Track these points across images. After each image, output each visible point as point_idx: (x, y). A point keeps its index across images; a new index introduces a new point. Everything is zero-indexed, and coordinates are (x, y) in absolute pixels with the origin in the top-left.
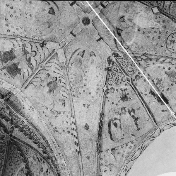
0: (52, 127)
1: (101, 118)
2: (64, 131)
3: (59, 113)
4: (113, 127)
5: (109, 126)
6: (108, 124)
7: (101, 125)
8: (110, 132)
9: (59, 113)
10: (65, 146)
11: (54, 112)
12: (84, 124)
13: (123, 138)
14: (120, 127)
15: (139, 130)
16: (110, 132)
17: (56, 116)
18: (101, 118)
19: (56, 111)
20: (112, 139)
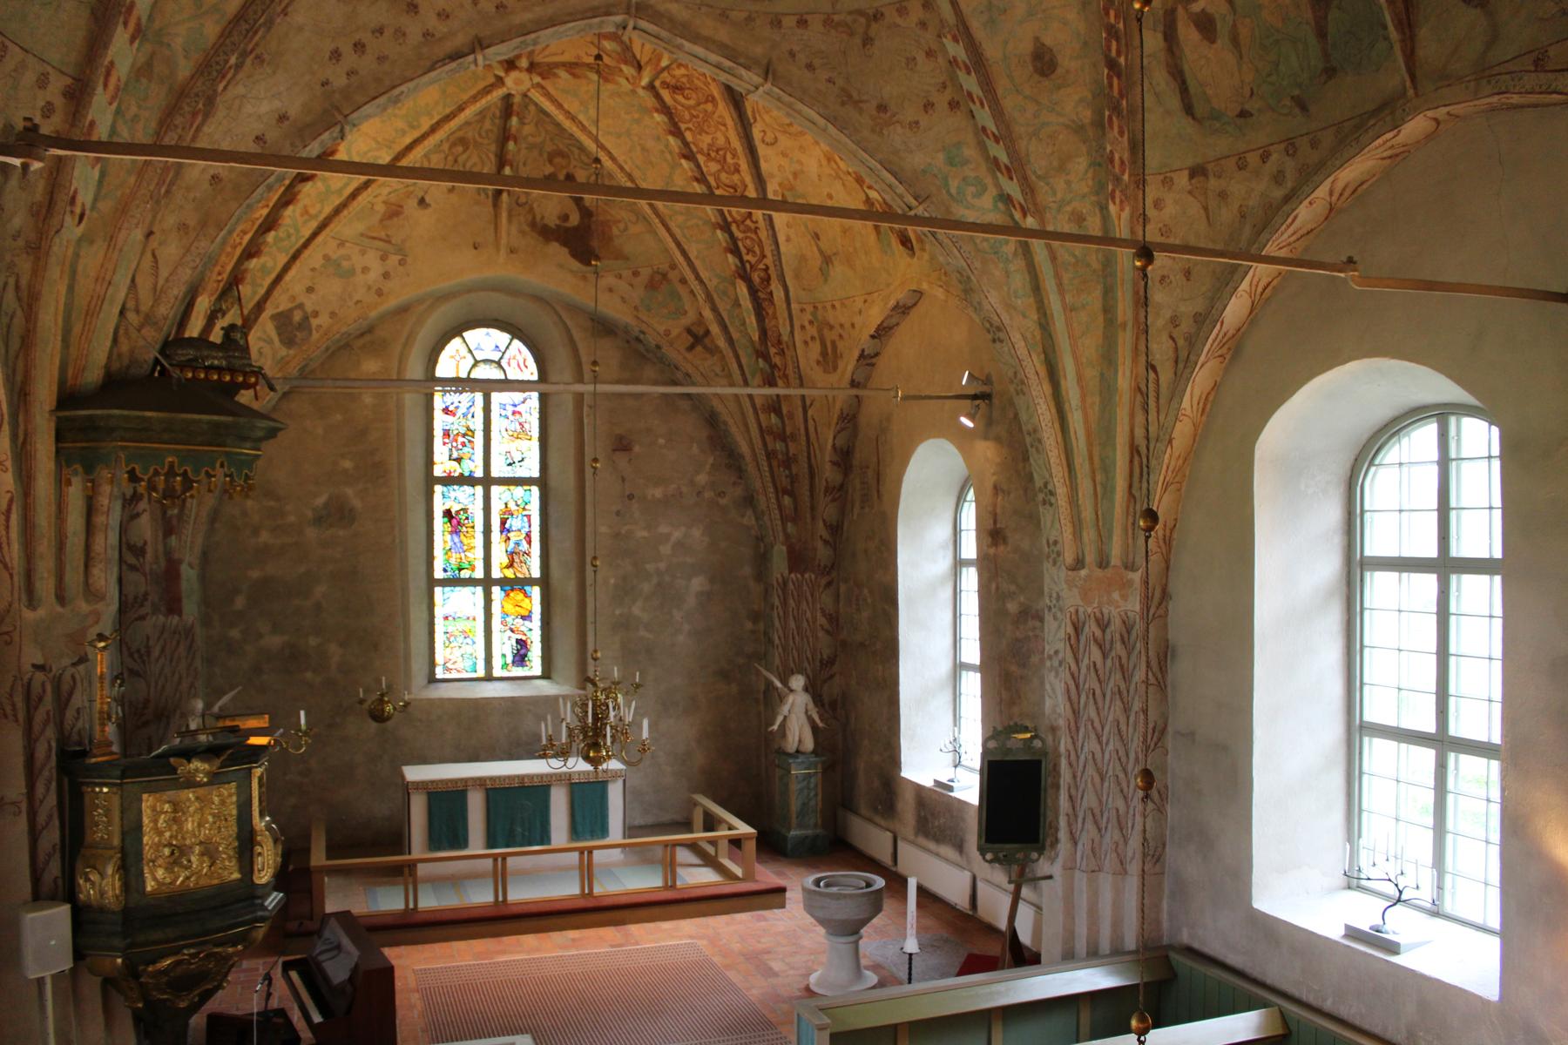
0: (861, 111)
1: (1112, 13)
2: (928, 106)
3: (877, 16)
4: (1188, 34)
5: (1170, 36)
6: (1161, 28)
7: (1114, 53)
8: (1178, 75)
9: (877, 16)
10: (954, 185)
11: (849, 19)
12: (1026, 47)
13: (1247, 107)
14: (1235, 40)
15: (1330, 78)
16: (1178, 75)
17: (867, 41)
18: (1107, 14)
19: (860, 12)
20: (1189, 109)
